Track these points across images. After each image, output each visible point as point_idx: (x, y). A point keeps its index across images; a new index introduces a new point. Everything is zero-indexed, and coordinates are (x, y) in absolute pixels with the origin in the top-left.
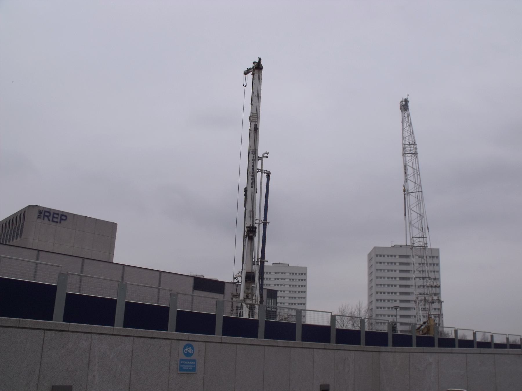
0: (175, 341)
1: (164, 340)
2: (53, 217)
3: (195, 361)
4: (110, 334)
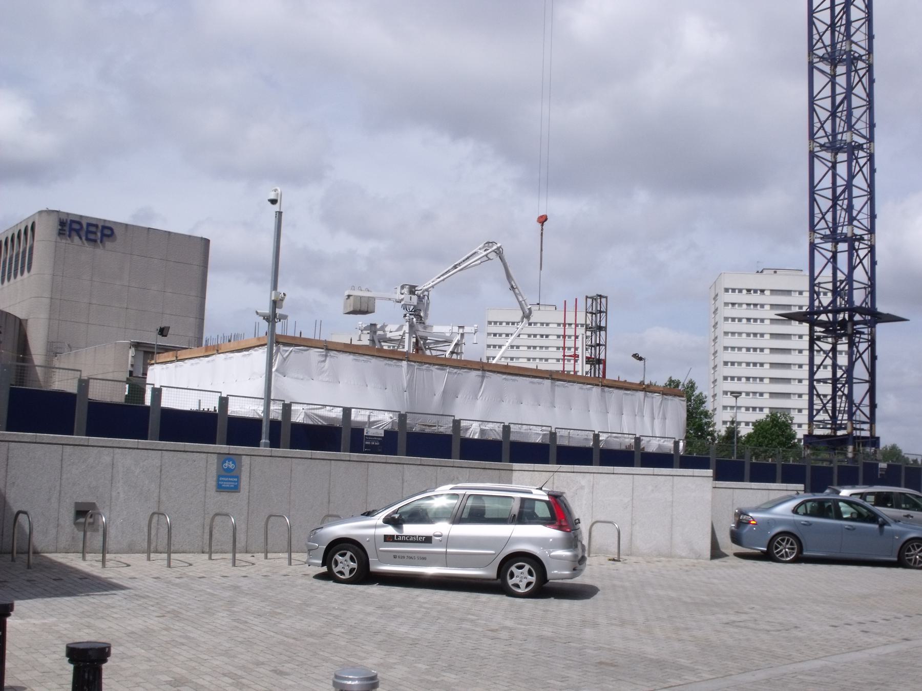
0: (212, 455)
2: (88, 232)
4: (134, 448)
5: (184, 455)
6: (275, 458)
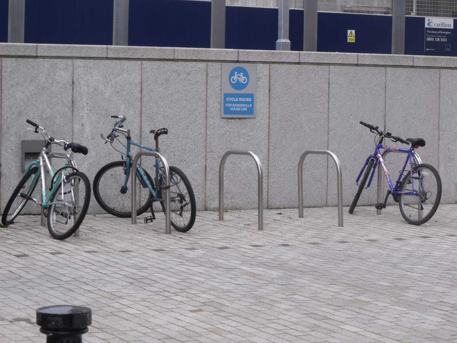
0: (214, 64)
1: (194, 63)
3: (251, 96)
4: (102, 58)
5: (174, 65)
6: (304, 66)
